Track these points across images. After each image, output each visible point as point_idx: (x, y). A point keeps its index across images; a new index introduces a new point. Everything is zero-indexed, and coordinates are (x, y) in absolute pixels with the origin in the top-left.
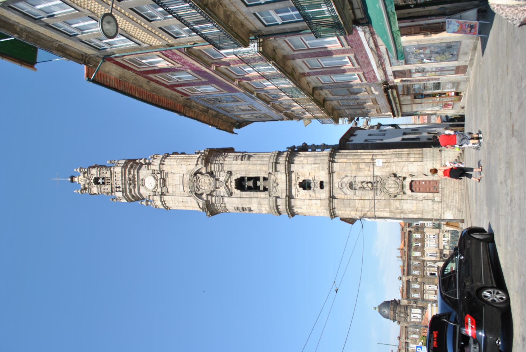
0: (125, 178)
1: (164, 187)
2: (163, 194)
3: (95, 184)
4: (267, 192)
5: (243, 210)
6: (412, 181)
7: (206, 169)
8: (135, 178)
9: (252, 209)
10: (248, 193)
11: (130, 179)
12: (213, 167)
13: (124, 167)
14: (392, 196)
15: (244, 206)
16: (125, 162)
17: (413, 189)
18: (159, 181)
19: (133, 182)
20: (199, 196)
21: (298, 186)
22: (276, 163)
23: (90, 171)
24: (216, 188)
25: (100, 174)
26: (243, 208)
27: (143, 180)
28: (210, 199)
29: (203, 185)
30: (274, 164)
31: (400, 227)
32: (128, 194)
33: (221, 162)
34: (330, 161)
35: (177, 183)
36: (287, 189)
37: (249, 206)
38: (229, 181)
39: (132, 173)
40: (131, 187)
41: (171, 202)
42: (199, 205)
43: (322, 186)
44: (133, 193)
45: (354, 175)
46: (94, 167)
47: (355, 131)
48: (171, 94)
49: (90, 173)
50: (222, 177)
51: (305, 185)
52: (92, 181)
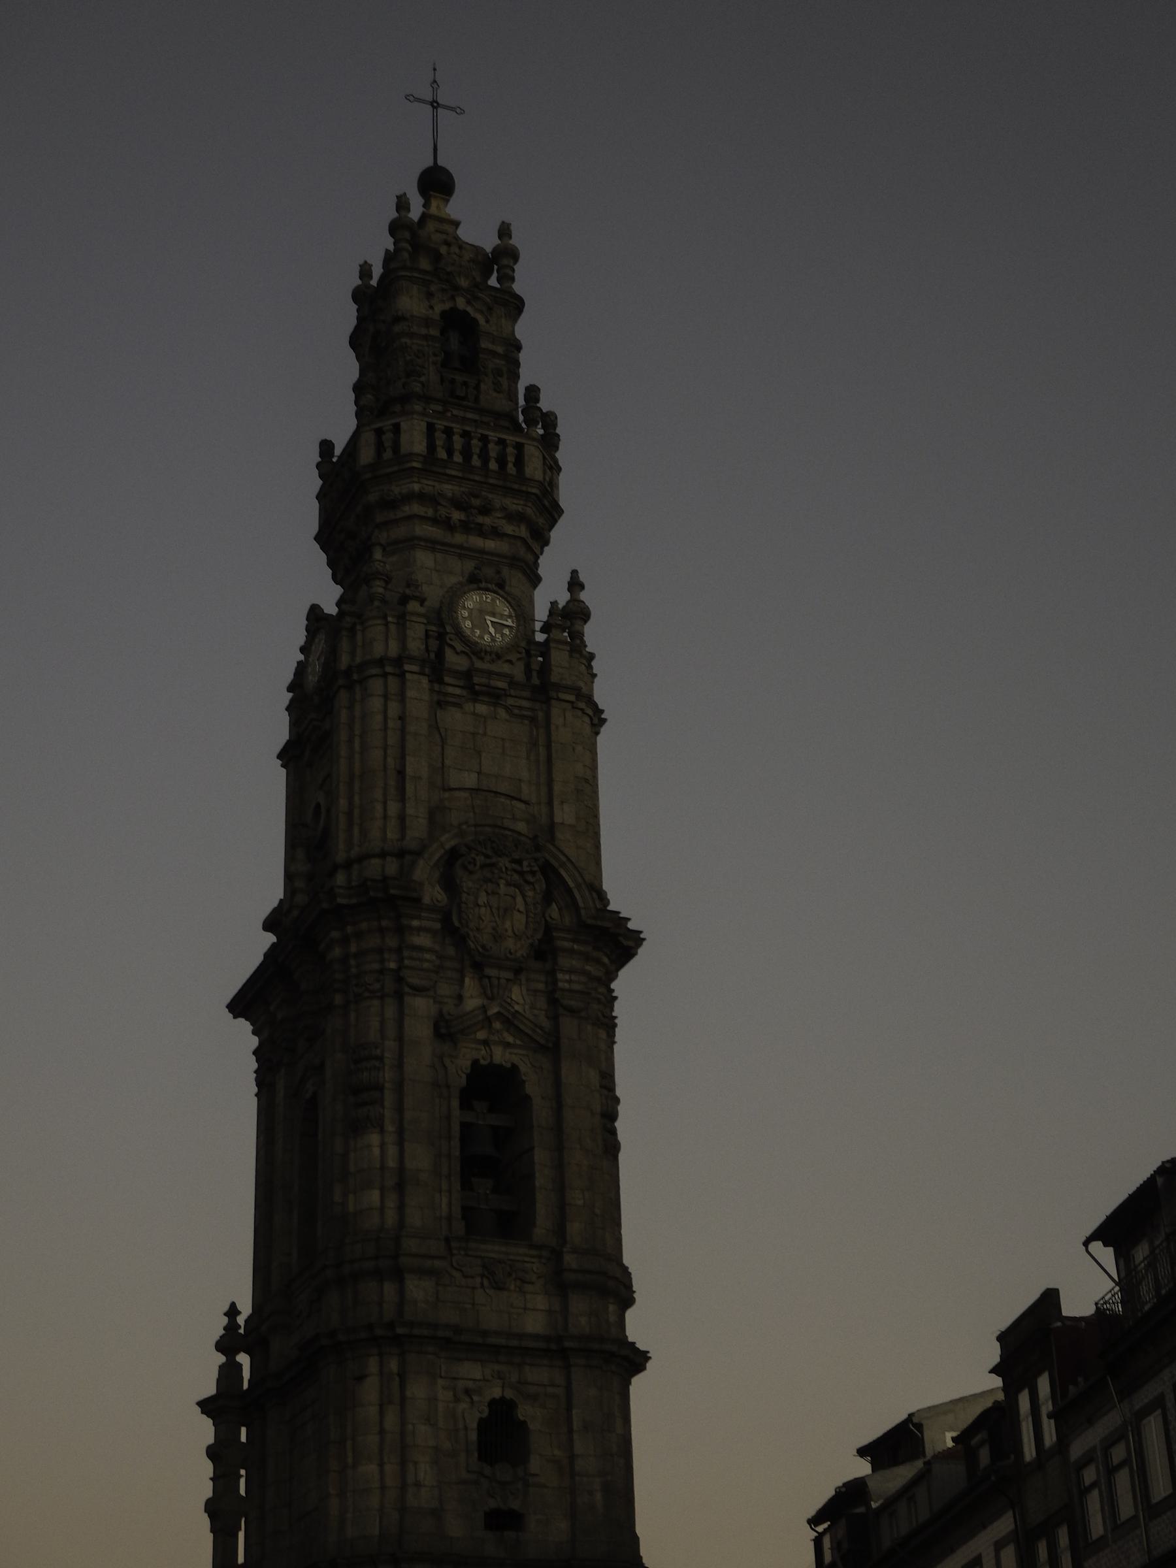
1: (470, 687)
2: (436, 669)
3: (444, 314)
9: (374, 1139)
10: (456, 1128)
11: (485, 510)
15: (389, 1098)
21: (497, 1392)
24: (478, 967)
25: (494, 354)
26: (381, 1089)
27: (501, 586)
32: (416, 487)
37: (390, 1127)
39: (509, 529)
42: (383, 855)
51: (501, 1436)
52: (461, 303)
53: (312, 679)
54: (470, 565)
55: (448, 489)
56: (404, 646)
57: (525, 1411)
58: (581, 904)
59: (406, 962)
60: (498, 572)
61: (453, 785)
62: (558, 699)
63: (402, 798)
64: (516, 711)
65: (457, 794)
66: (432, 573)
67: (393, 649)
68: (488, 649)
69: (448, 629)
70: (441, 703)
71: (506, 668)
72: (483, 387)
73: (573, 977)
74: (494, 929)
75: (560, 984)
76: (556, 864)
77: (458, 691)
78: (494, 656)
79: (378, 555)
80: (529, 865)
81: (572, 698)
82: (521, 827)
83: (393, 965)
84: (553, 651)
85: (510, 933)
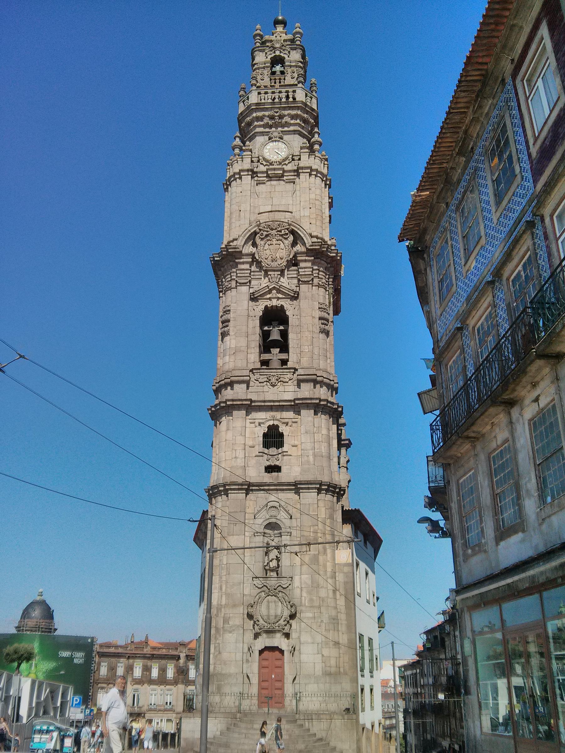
0: (284, 109)
1: (268, 176)
2: (253, 173)
4: (258, 365)
5: (223, 322)
6: (282, 652)
7: (302, 253)
8: (283, 126)
9: (227, 339)
11: (281, 117)
12: (306, 266)
13: (305, 107)
14: (250, 610)
16: (313, 110)
17: (266, 653)
18: (280, 166)
19: (276, 122)
20: (252, 238)
21: (271, 423)
22: (315, 382)
23: (295, 49)
24: (266, 272)
25: (291, 66)
26: (228, 321)
27: (281, 138)
28: (245, 260)
30: (314, 377)
31: (187, 640)
32: (254, 115)
33: (316, 281)
34: (321, 484)
35: (276, 201)
36: (264, 401)
37: (231, 333)
38: (280, 296)
39: (292, 122)
40: (266, 120)
41: (240, 189)
43: (271, 469)
44: (256, 123)
45: (294, 533)
46: (303, 57)
47: (372, 544)
48: (521, 28)
49: (292, 49)
50: (288, 282)
51: (273, 438)
52: (278, 53)
55: (267, 113)
57: (283, 429)
62: (303, 172)
69: (260, 158)
73: (306, 270)
75: (301, 273)
76: (296, 230)
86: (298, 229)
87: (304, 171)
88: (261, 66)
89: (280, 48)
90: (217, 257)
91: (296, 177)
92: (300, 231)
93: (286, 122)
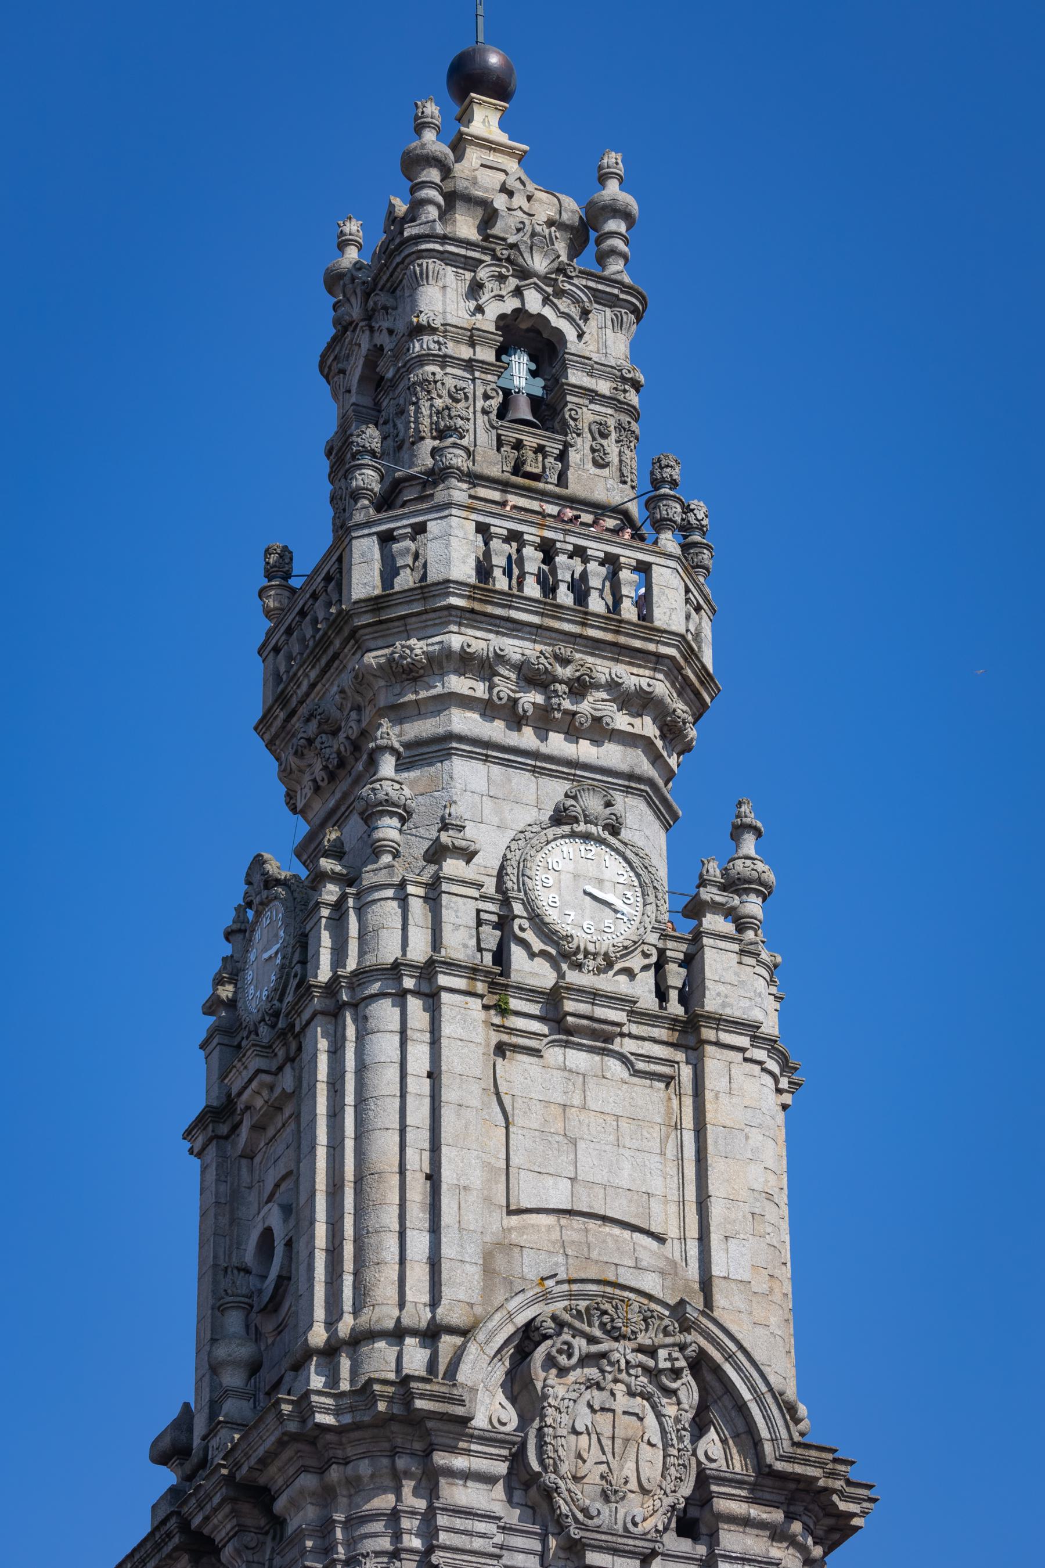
0: (596, 646)
8: (573, 731)
11: (579, 688)
19: (547, 701)
25: (593, 395)
27: (614, 830)
29: (603, 1422)
32: (456, 642)
39: (622, 721)
40: (505, 687)
42: (398, 1334)
49: (599, 297)
52: (533, 302)
53: (257, 994)
54: (555, 790)
55: (515, 648)
56: (436, 942)
58: (764, 1433)
59: (443, 1537)
60: (608, 804)
61: (525, 1204)
63: (435, 1229)
64: (641, 1065)
65: (533, 1218)
66: (491, 804)
67: (419, 950)
68: (591, 948)
69: (518, 909)
70: (501, 1049)
71: (621, 985)
72: (573, 456)
74: (602, 1477)
77: (536, 1026)
78: (600, 960)
79: (387, 766)
80: (670, 1358)
81: (744, 1041)
82: (651, 1283)
83: (416, 1543)
84: (709, 955)
85: (633, 1485)
86: (729, 1357)
87: (726, 1038)
88: (451, 349)
89: (545, 279)
90: (327, 1411)
91: (680, 1056)
92: (738, 1369)
93: (597, 720)
